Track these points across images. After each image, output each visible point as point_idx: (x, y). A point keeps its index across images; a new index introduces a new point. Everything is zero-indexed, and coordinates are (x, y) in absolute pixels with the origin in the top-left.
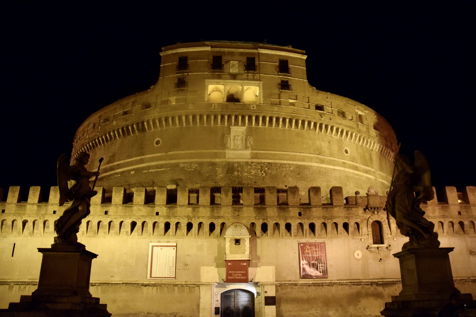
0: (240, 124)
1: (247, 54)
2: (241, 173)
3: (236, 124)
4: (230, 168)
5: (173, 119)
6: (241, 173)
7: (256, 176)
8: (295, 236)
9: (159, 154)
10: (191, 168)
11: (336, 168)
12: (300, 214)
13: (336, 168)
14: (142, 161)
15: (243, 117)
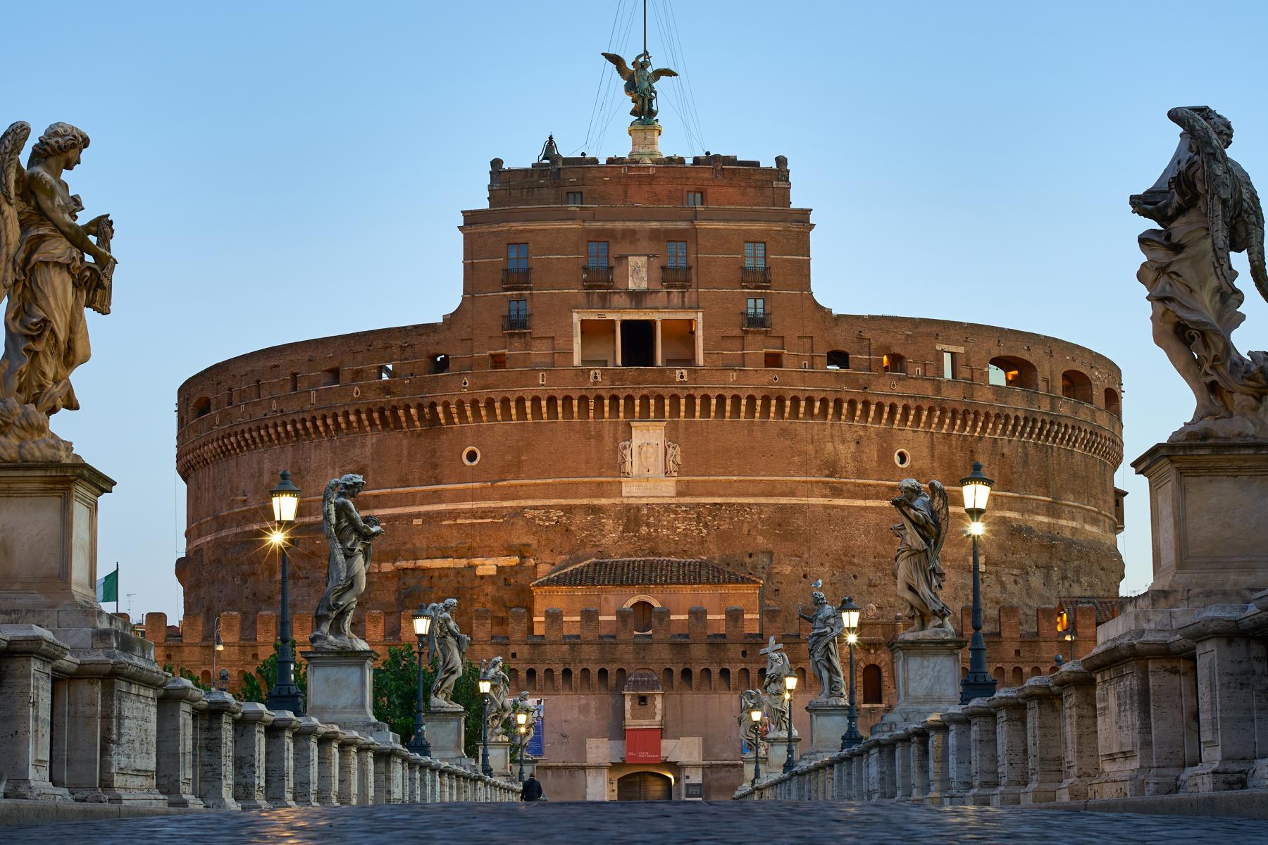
0: (652, 414)
1: (667, 231)
2: (656, 531)
3: (645, 415)
4: (632, 517)
5: (505, 402)
6: (656, 531)
7: (686, 535)
8: (736, 689)
9: (477, 485)
10: (549, 519)
11: (870, 503)
12: (744, 653)
13: (870, 503)
14: (437, 497)
15: (660, 399)
